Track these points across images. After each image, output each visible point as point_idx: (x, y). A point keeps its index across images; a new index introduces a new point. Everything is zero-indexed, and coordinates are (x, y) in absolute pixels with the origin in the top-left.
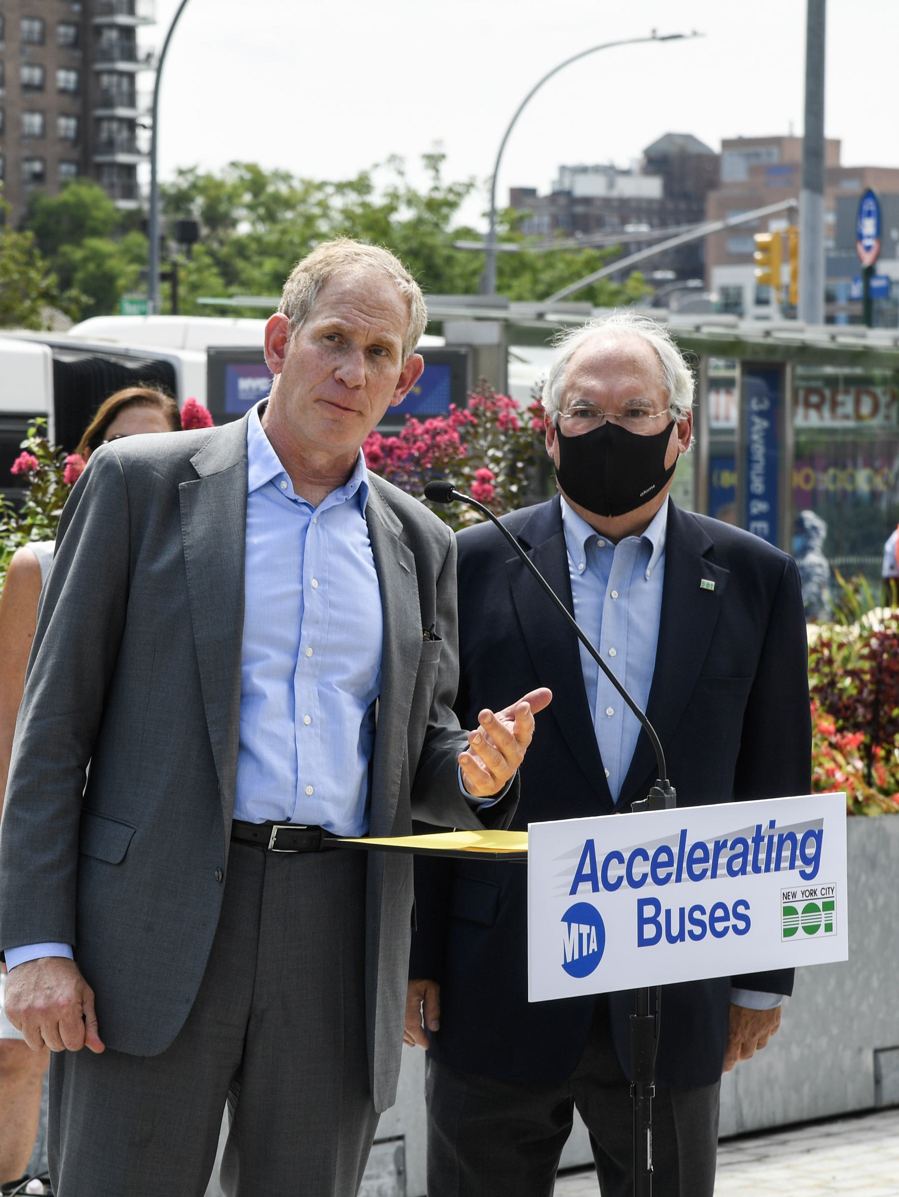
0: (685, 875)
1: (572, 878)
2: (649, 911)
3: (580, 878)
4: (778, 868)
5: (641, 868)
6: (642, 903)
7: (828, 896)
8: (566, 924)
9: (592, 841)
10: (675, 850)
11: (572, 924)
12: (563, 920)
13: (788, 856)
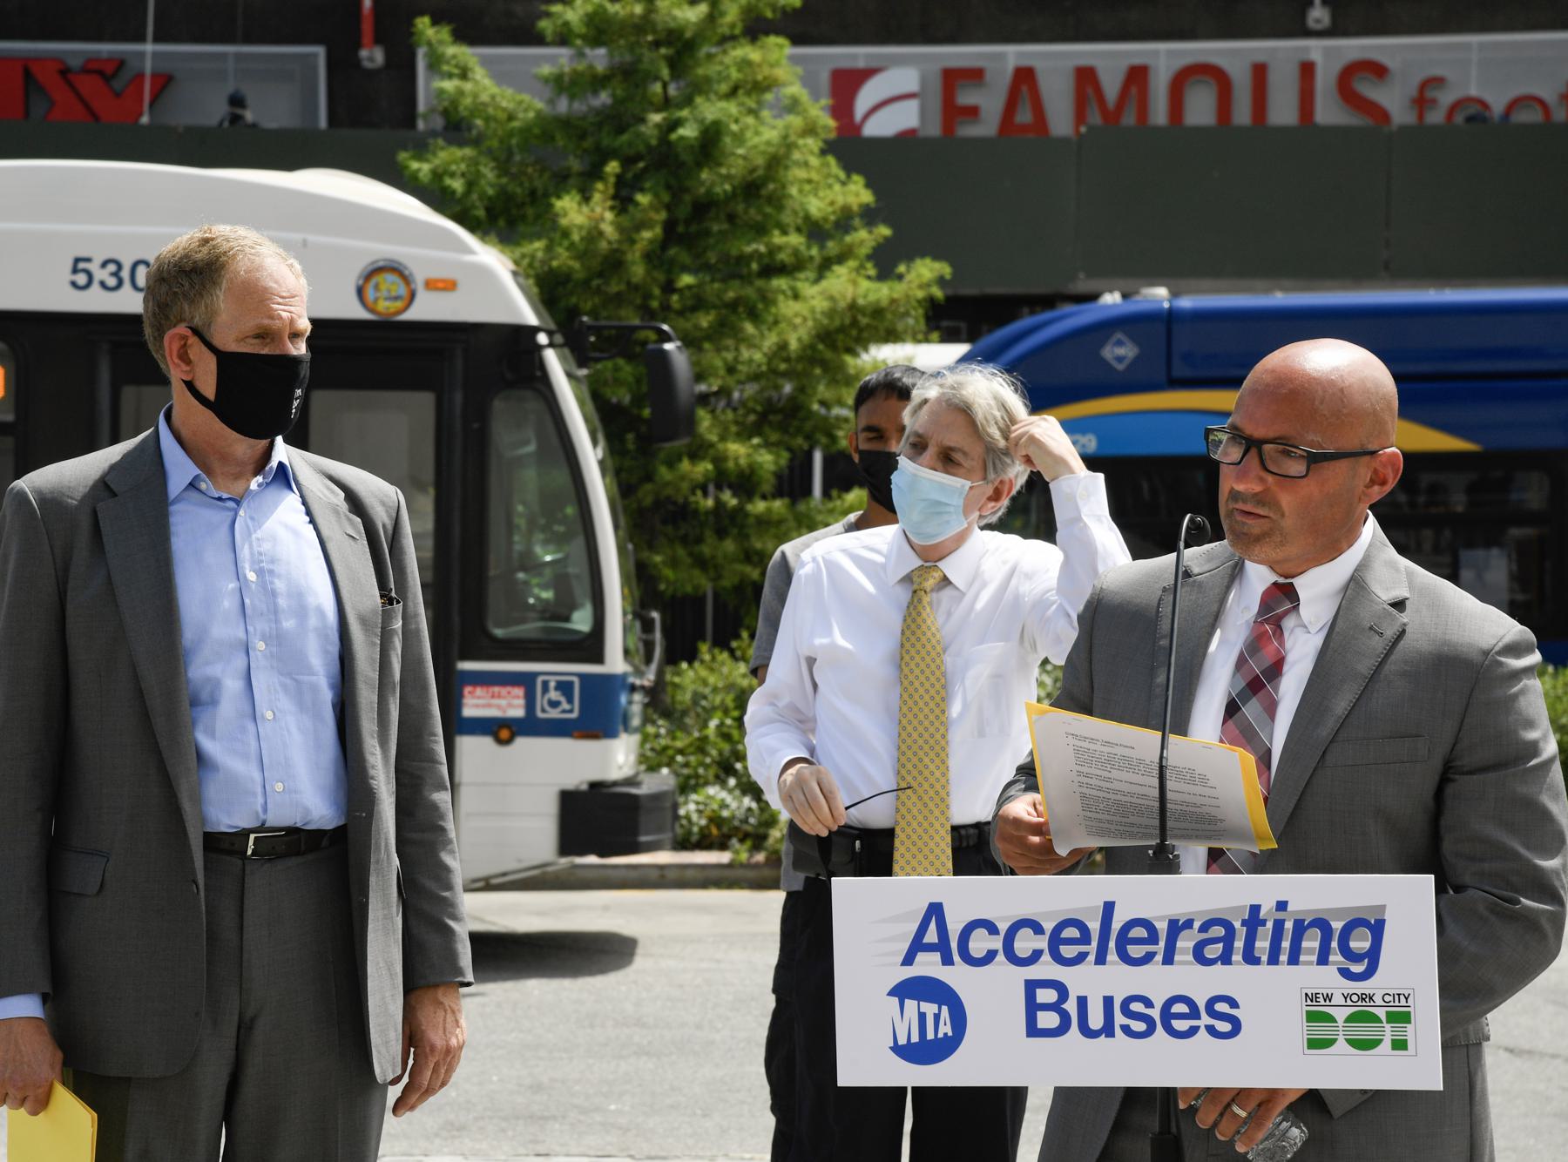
0: (1112, 956)
1: (906, 946)
3: (917, 946)
4: (1294, 960)
5: (1025, 943)
6: (1031, 986)
7: (1397, 1004)
8: (896, 1000)
9: (940, 905)
10: (1094, 926)
11: (906, 1000)
12: (891, 993)
13: (1315, 948)
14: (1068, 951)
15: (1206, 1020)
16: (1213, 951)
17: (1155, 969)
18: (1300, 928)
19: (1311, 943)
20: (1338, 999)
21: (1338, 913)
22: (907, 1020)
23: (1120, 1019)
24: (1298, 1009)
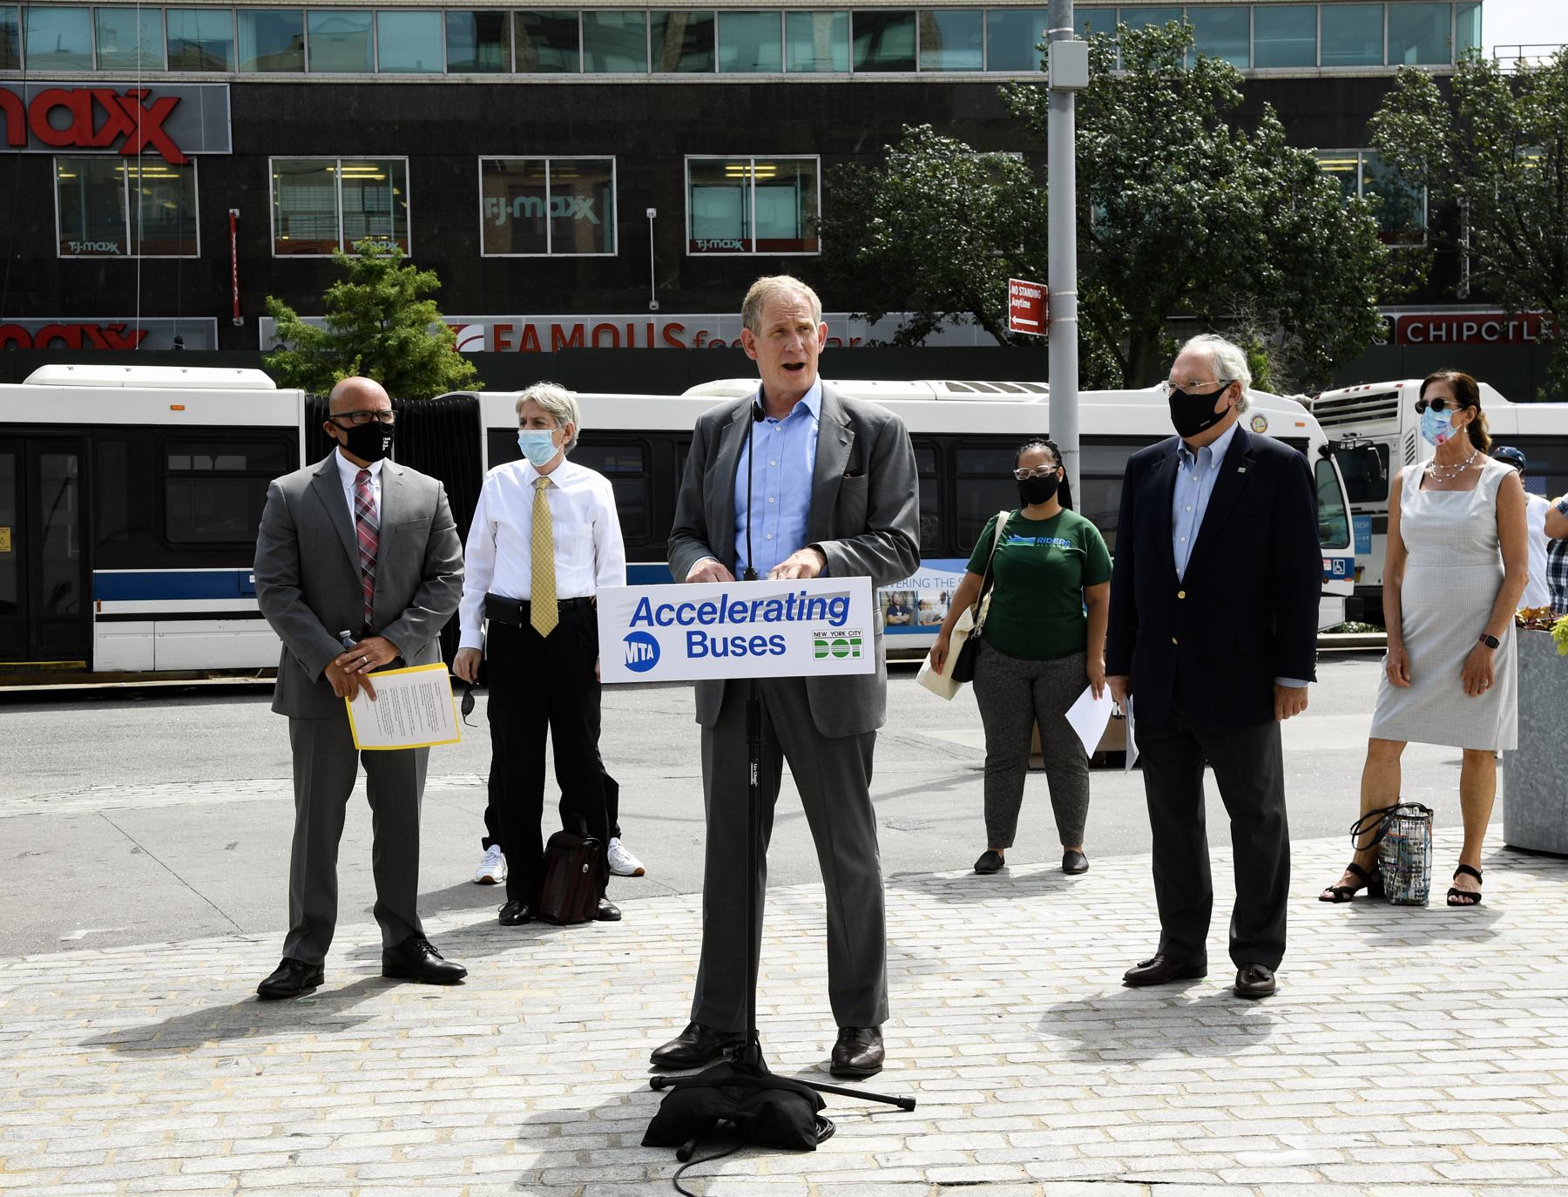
0: (727, 619)
2: (697, 638)
3: (637, 617)
4: (809, 618)
6: (690, 634)
10: (718, 606)
14: (706, 618)
15: (770, 646)
16: (773, 615)
17: (747, 623)
18: (812, 603)
19: (817, 609)
20: (829, 635)
21: (828, 595)
22: (632, 652)
23: (730, 648)
24: (813, 639)
